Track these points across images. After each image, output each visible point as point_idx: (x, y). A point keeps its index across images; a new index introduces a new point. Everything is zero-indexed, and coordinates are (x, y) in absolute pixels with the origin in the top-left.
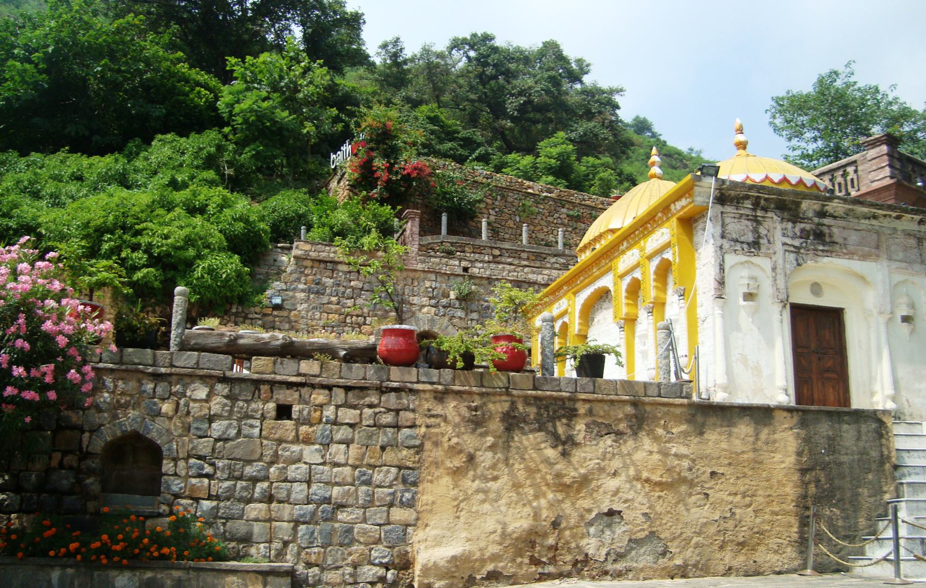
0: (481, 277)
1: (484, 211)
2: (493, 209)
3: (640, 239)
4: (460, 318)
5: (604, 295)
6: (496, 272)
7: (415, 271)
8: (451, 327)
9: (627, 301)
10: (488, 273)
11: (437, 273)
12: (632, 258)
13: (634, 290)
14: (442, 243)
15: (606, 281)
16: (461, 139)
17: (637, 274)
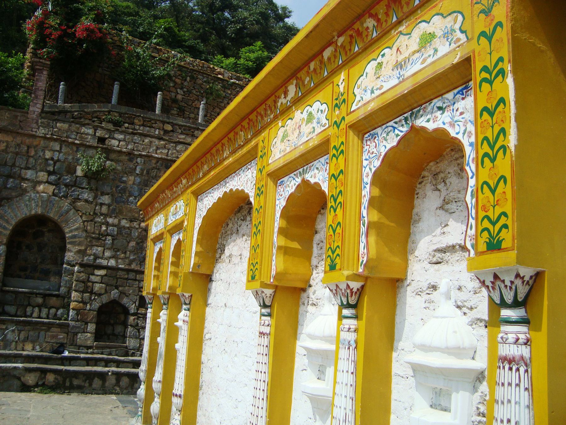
0: (120, 152)
1: (173, 89)
2: (182, 89)
3: (334, 72)
4: (86, 201)
5: (238, 209)
6: (140, 147)
7: (34, 137)
8: (73, 211)
9: (283, 242)
10: (130, 147)
11: (62, 142)
12: (306, 129)
13: (308, 210)
14: (109, 112)
15: (245, 182)
16: (187, 47)
17: (318, 176)
